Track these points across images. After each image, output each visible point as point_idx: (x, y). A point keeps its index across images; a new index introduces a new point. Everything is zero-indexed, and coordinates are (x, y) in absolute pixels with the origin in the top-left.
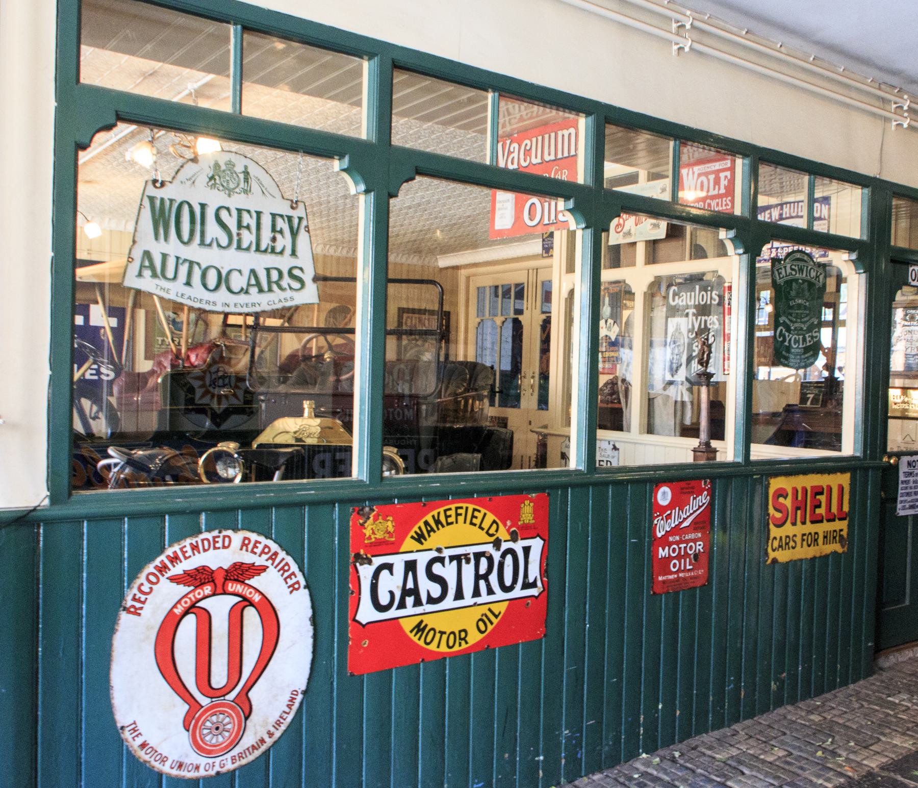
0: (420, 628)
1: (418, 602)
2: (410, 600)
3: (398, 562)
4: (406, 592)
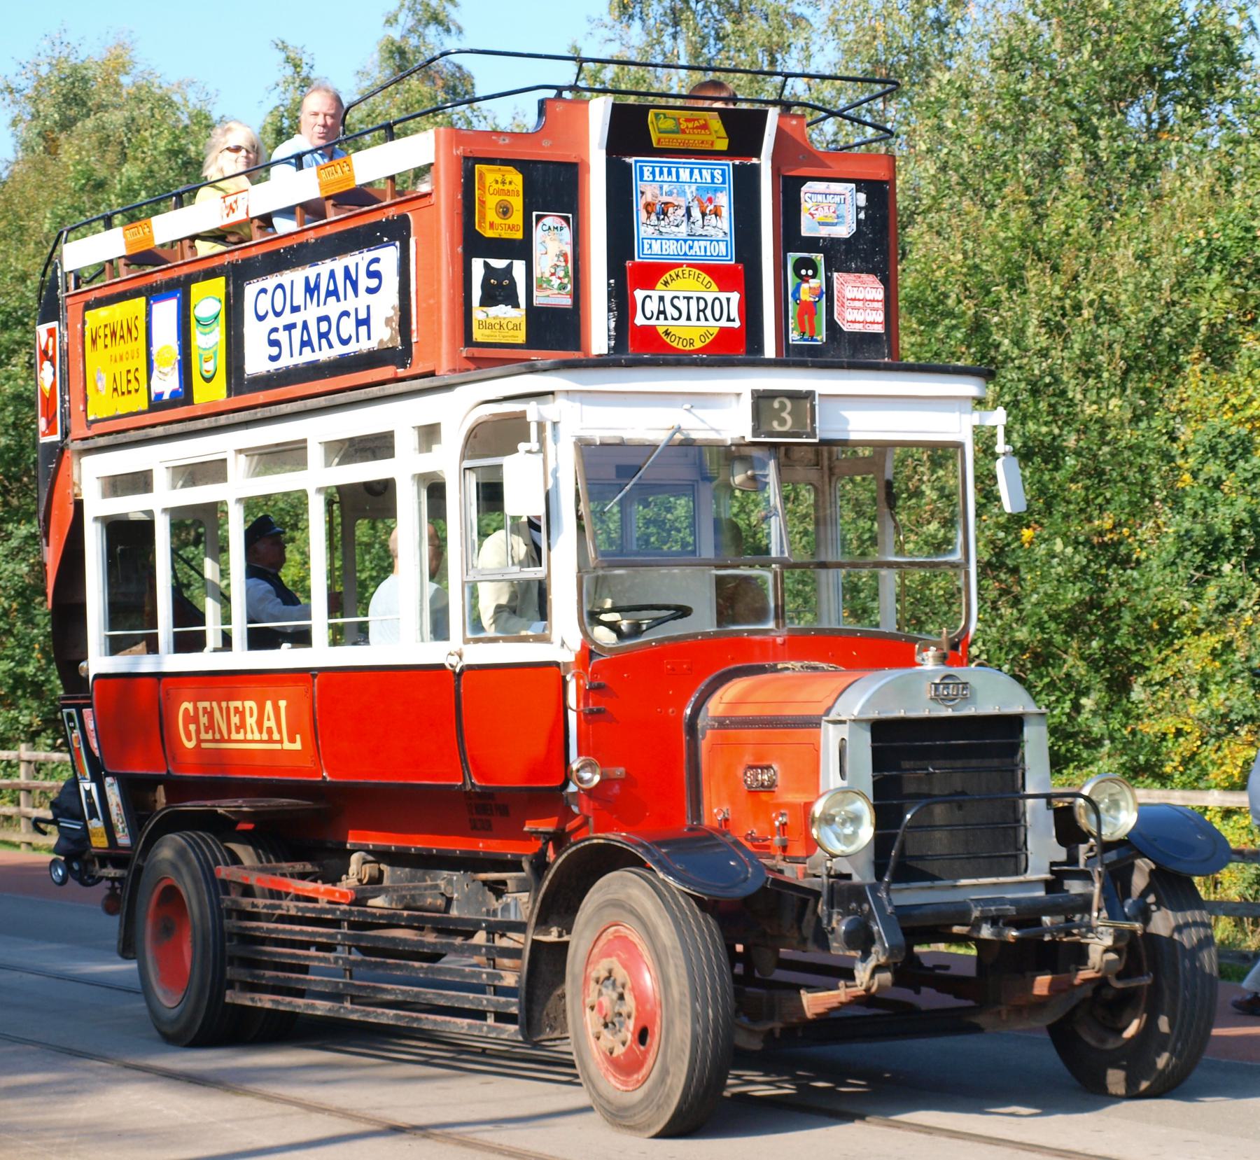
0: (667, 333)
1: (666, 319)
2: (662, 317)
3: (655, 294)
4: (660, 312)
